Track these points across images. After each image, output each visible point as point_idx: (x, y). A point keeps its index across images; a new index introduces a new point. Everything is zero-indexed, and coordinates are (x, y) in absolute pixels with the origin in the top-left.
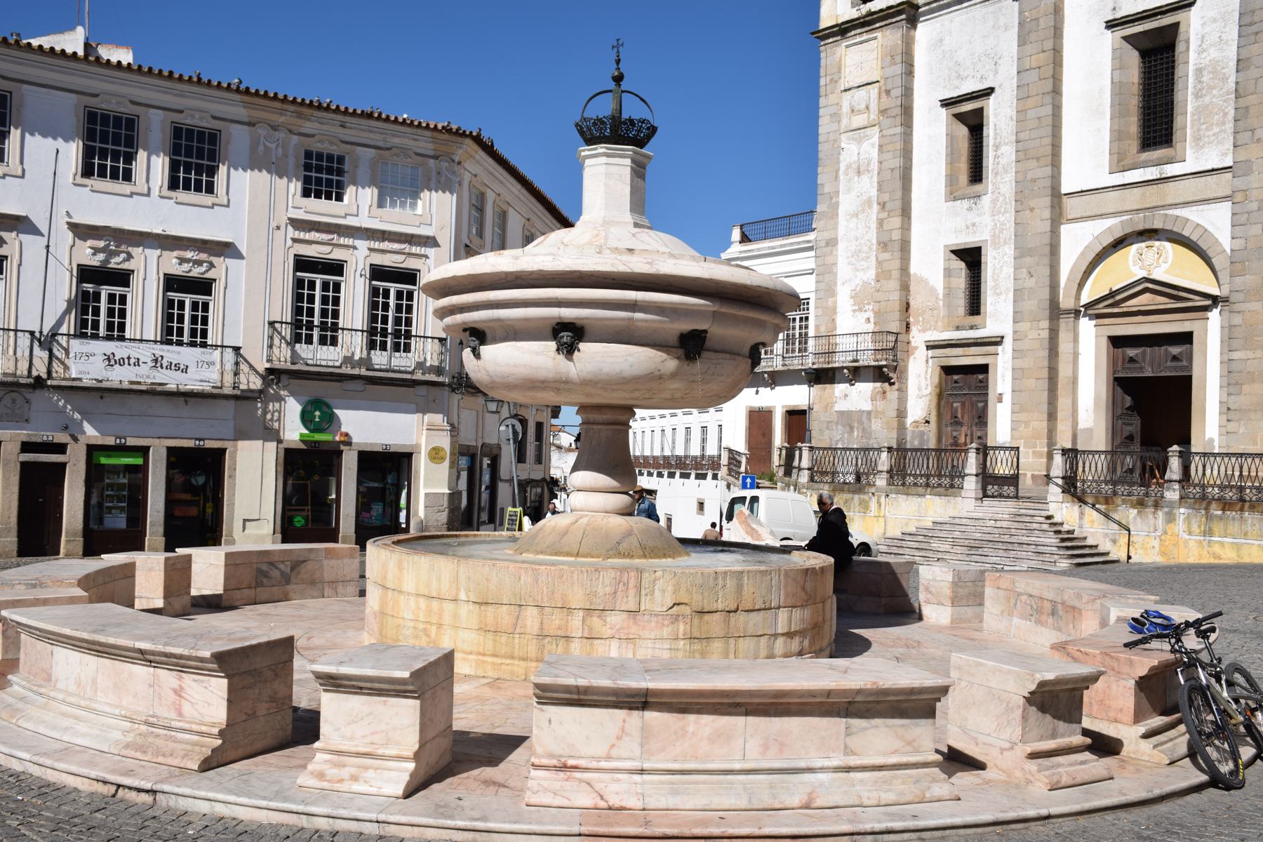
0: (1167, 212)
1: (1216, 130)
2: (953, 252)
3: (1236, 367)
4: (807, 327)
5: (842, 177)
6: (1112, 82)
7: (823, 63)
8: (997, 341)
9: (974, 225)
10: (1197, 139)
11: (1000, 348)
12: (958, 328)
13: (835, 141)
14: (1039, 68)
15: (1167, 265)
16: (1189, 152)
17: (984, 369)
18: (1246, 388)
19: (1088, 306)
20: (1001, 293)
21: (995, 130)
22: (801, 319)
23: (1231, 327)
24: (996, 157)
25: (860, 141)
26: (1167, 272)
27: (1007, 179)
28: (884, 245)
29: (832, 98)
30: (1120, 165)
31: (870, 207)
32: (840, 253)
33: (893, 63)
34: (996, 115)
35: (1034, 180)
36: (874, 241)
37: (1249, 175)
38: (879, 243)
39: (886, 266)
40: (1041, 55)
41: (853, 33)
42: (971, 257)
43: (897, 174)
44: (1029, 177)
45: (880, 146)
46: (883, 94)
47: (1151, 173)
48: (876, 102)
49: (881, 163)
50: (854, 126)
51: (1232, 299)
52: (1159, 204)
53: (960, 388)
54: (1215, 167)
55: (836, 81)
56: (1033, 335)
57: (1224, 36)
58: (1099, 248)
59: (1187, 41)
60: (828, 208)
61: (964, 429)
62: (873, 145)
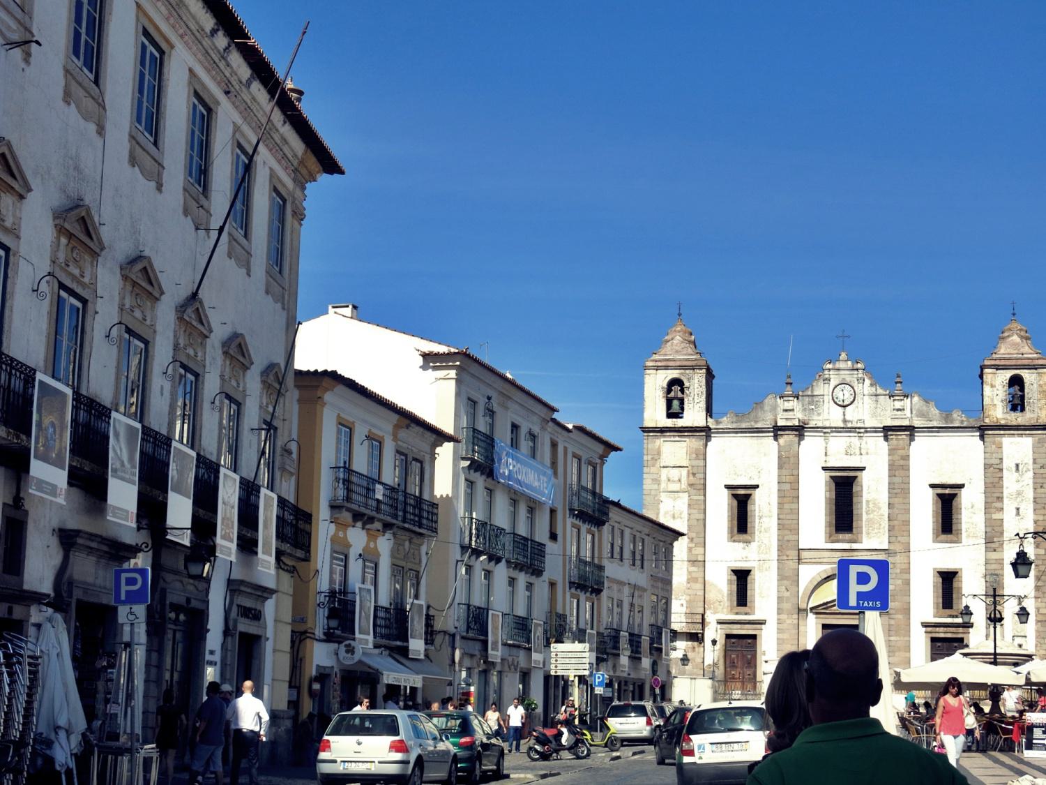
3: (892, 644)
7: (645, 446)
8: (762, 623)
10: (868, 534)
11: (763, 626)
12: (737, 614)
13: (656, 495)
17: (754, 637)
19: (811, 609)
29: (653, 470)
30: (830, 539)
33: (697, 458)
35: (788, 541)
39: (694, 575)
41: (668, 434)
42: (742, 576)
44: (785, 539)
45: (689, 505)
46: (691, 475)
50: (669, 490)
53: (736, 647)
56: (789, 621)
61: (739, 670)
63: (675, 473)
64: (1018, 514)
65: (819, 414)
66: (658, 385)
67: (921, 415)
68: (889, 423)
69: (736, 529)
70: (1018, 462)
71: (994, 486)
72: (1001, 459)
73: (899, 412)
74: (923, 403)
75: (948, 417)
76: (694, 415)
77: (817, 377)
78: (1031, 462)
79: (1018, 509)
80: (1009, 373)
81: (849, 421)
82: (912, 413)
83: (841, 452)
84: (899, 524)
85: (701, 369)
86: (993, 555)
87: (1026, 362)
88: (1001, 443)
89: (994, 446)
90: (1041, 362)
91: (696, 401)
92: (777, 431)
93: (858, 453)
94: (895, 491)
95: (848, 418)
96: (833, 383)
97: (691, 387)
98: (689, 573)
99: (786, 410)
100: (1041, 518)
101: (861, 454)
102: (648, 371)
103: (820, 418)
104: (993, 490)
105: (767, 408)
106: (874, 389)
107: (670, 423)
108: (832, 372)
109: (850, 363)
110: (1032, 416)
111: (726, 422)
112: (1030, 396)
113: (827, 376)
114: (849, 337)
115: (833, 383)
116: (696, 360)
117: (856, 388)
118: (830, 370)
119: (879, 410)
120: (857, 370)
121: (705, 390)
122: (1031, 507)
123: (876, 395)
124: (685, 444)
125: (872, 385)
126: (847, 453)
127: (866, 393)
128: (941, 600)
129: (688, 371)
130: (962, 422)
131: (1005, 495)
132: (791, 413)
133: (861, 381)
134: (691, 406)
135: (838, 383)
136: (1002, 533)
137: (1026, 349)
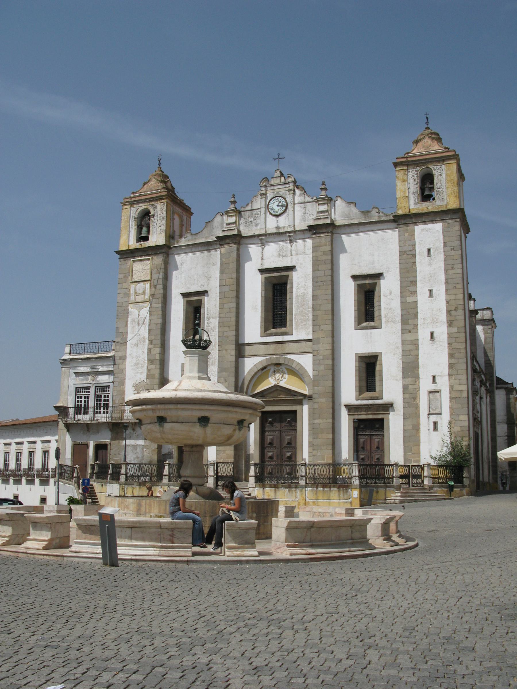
0: (285, 356)
4: (108, 400)
5: (129, 325)
6: (261, 296)
14: (230, 285)
15: (285, 380)
16: (294, 331)
18: (320, 436)
21: (208, 311)
22: (105, 397)
23: (314, 409)
24: (208, 323)
25: (140, 309)
26: (285, 383)
27: (213, 334)
28: (151, 361)
29: (125, 285)
31: (144, 341)
32: (127, 363)
35: (227, 337)
36: (146, 359)
37: (319, 344)
38: (149, 360)
39: (152, 372)
40: (231, 280)
43: (159, 326)
44: (225, 334)
45: (150, 312)
46: (152, 287)
49: (150, 320)
50: (137, 300)
51: (313, 397)
52: (282, 352)
54: (305, 339)
55: (127, 277)
57: (306, 284)
58: (256, 370)
59: (292, 283)
60: (121, 340)
65: (257, 225)
70: (429, 247)
71: (408, 272)
72: (414, 245)
78: (442, 245)
79: (431, 291)
85: (163, 199)
86: (409, 337)
89: (407, 234)
91: (159, 225)
93: (289, 254)
94: (318, 284)
98: (149, 370)
100: (453, 297)
101: (292, 255)
107: (138, 245)
109: (283, 179)
114: (283, 158)
117: (287, 199)
121: (165, 215)
122: (443, 288)
123: (305, 203)
124: (149, 262)
126: (279, 256)
129: (153, 203)
131: (418, 278)
135: (272, 197)
136: (416, 316)
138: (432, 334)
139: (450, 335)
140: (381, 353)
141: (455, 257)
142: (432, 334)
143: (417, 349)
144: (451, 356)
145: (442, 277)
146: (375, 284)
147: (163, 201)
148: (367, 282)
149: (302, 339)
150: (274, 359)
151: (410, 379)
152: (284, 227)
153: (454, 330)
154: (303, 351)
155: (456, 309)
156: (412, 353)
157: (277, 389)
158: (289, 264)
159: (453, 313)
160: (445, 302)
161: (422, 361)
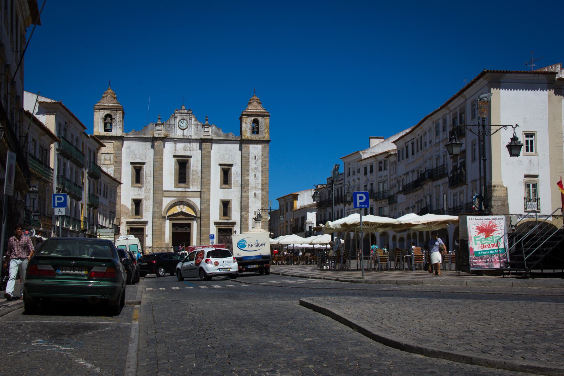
0: (187, 198)
1: (196, 183)
2: (133, 200)
9: (140, 194)
10: (193, 184)
12: (135, 219)
16: (191, 187)
19: (168, 216)
20: (147, 211)
25: (108, 168)
34: (146, 169)
35: (159, 187)
45: (114, 171)
47: (183, 190)
48: (113, 159)
50: (105, 164)
56: (158, 222)
62: (112, 170)
63: (108, 156)
64: (255, 177)
65: (172, 132)
66: (100, 116)
67: (216, 134)
68: (204, 137)
69: (135, 182)
71: (246, 165)
73: (207, 133)
74: (216, 129)
75: (227, 136)
76: (117, 131)
77: (172, 116)
79: (255, 175)
80: (253, 118)
81: (185, 136)
82: (212, 133)
83: (181, 149)
84: (205, 180)
87: (260, 114)
88: (249, 147)
89: (246, 148)
90: (266, 114)
91: (118, 124)
92: (154, 139)
95: (185, 134)
96: (178, 119)
97: (116, 118)
99: (158, 130)
101: (190, 150)
102: (96, 110)
103: (173, 134)
104: (245, 167)
105: (149, 129)
106: (196, 122)
107: (106, 134)
108: (178, 114)
110: (262, 136)
111: (131, 135)
112: (261, 127)
113: (176, 116)
115: (178, 119)
116: (117, 106)
117: (188, 122)
118: (177, 113)
119: (198, 132)
120: (189, 114)
121: (122, 120)
122: (261, 173)
123: (197, 125)
124: (113, 144)
125: (195, 121)
126: (184, 150)
127: (193, 124)
128: (222, 213)
129: (114, 111)
130: (233, 138)
131: (250, 169)
132: (160, 131)
133: (191, 119)
134: (115, 127)
135: (180, 119)
136: (248, 185)
137: (260, 108)
138: (255, 193)
139: (262, 194)
140: (231, 200)
141: (266, 161)
142: (255, 193)
143: (248, 200)
144: (262, 204)
145: (261, 170)
146: (229, 169)
147: (120, 111)
148: (226, 167)
149: (195, 190)
150: (181, 199)
151: (245, 212)
152: (186, 136)
153: (265, 193)
154: (195, 196)
155: (265, 184)
156: (246, 201)
157: (182, 213)
158: (189, 155)
159: (264, 185)
160: (261, 180)
161: (250, 205)
